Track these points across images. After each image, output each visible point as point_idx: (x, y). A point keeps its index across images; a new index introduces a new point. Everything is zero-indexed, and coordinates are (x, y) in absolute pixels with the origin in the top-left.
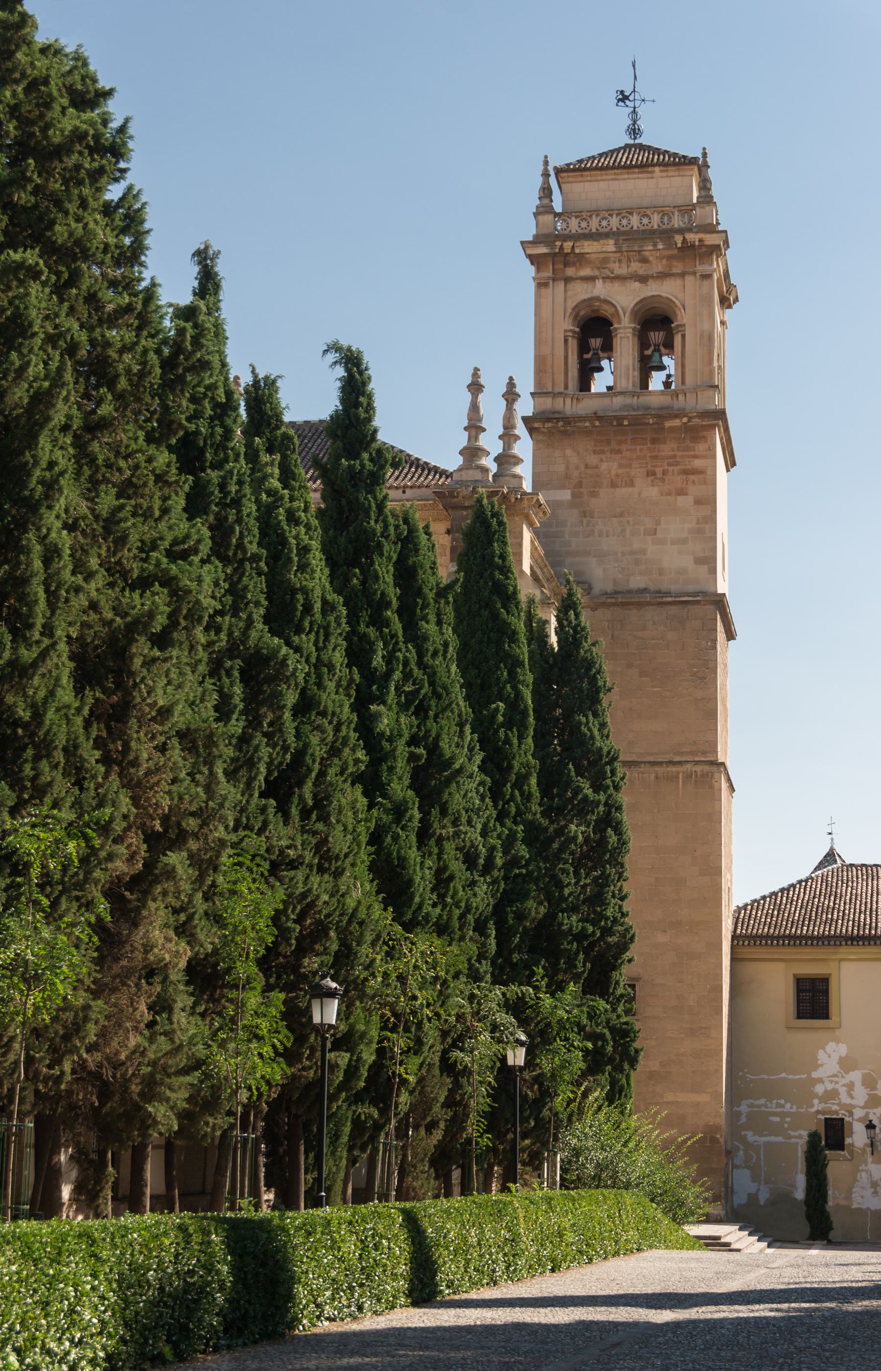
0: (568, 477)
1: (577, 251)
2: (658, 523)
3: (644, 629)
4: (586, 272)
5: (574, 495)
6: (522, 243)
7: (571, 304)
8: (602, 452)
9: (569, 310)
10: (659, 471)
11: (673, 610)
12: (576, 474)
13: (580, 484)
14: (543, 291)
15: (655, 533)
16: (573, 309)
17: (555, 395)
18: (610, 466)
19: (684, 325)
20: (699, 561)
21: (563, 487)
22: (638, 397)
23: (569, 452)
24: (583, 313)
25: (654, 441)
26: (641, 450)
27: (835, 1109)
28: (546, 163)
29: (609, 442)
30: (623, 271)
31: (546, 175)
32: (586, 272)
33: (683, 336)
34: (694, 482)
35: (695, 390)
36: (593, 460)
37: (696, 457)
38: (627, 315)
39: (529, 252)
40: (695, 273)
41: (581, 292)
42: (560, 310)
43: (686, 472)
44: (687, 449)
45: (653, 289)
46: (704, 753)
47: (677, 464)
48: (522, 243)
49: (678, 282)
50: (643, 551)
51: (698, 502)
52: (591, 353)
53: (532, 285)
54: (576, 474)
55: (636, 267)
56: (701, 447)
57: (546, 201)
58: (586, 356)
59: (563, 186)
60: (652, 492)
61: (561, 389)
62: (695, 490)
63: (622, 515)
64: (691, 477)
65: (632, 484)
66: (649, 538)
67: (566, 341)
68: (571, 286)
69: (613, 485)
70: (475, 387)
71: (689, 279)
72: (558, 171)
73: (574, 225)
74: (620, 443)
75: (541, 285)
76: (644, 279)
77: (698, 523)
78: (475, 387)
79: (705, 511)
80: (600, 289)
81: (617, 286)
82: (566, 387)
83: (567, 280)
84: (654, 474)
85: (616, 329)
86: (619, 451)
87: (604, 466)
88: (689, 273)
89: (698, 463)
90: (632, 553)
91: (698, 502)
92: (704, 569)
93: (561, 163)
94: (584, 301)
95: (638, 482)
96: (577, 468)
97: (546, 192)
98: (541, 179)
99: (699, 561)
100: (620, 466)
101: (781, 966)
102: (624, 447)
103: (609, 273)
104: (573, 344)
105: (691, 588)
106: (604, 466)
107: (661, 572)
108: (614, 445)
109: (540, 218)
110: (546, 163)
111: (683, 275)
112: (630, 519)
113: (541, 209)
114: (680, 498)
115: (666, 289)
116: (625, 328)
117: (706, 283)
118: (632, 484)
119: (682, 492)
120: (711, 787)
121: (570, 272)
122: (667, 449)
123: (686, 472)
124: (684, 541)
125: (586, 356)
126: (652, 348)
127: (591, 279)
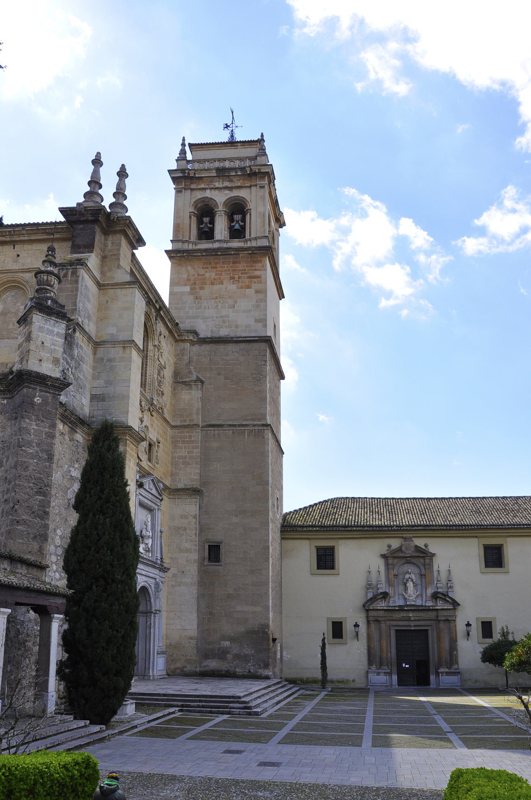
0: (188, 280)
2: (236, 302)
3: (227, 355)
5: (191, 289)
6: (169, 171)
7: (193, 200)
8: (207, 268)
9: (192, 203)
10: (236, 277)
11: (242, 346)
12: (192, 278)
13: (195, 284)
14: (179, 194)
15: (234, 307)
16: (194, 202)
17: (183, 242)
18: (211, 274)
19: (251, 209)
20: (257, 321)
21: (186, 285)
22: (227, 243)
23: (189, 268)
24: (199, 205)
25: (234, 263)
26: (227, 267)
27: (337, 616)
28: (184, 139)
31: (183, 145)
33: (250, 214)
34: (255, 282)
35: (256, 239)
36: (202, 272)
37: (256, 270)
38: (222, 205)
39: (173, 176)
40: (256, 185)
41: (199, 195)
43: (250, 277)
44: (251, 266)
45: (236, 193)
46: (259, 420)
47: (246, 273)
48: (170, 171)
49: (248, 190)
50: (228, 316)
51: (257, 292)
52: (204, 224)
53: (174, 192)
54: (192, 278)
56: (258, 266)
57: (183, 156)
58: (201, 226)
59: (193, 152)
60: (233, 287)
62: (255, 286)
63: (216, 298)
64: (254, 280)
65: (222, 284)
66: (231, 310)
67: (190, 217)
69: (212, 284)
70: (97, 162)
71: (253, 189)
72: (190, 145)
73: (197, 166)
74: (216, 263)
75: (178, 191)
76: (230, 189)
77: (257, 302)
78: (97, 162)
79: (261, 296)
80: (208, 194)
81: (217, 192)
82: (190, 239)
83: (192, 190)
84: (234, 278)
85: (216, 212)
87: (207, 275)
88: (253, 186)
89: (257, 273)
90: (222, 317)
91: (257, 292)
92: (260, 324)
93: (192, 142)
94: (200, 199)
95: (225, 282)
96: (193, 275)
97: (183, 152)
98: (181, 147)
99: (257, 321)
100: (216, 275)
101: (307, 542)
102: (218, 266)
103: (213, 187)
104: (194, 219)
105: (253, 335)
106: (207, 275)
107: (237, 326)
108: (213, 265)
109: (179, 162)
110: (184, 139)
111: (250, 187)
112: (221, 300)
113: (180, 158)
114: (247, 290)
115: (243, 193)
116: (220, 211)
117: (262, 190)
118: (222, 284)
119: (249, 287)
120: (263, 437)
121: (193, 186)
122: (241, 266)
123: (250, 277)
124: (249, 311)
125: (201, 226)
126: (235, 222)
127: (205, 189)
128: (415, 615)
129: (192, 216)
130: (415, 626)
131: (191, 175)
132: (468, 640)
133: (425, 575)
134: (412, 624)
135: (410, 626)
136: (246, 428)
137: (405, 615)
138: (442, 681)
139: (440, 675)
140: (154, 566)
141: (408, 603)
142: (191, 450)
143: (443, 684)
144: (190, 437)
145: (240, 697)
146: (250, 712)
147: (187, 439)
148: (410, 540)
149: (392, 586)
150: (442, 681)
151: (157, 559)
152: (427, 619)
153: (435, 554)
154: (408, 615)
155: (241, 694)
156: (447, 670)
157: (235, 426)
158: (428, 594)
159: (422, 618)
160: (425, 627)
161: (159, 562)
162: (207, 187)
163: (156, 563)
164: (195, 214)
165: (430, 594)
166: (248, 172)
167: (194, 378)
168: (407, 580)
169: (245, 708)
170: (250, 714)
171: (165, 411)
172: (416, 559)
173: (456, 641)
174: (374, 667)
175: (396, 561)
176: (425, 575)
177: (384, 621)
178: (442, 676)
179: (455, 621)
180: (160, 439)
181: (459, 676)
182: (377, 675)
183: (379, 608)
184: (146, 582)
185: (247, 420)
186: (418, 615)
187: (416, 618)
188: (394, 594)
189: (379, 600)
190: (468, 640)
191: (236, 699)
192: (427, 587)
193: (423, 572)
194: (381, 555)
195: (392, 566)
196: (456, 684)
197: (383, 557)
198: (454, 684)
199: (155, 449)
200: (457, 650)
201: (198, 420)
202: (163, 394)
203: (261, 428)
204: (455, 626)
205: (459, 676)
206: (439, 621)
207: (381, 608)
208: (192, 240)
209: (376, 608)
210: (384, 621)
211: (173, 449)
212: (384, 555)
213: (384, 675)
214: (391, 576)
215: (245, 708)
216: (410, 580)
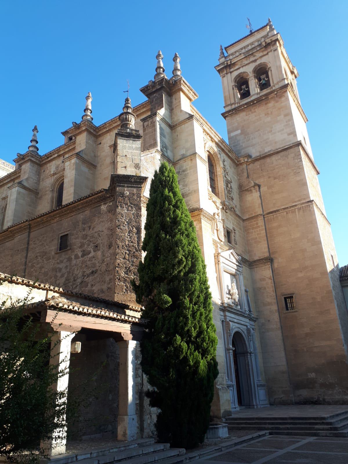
1: (232, 63)
4: (237, 67)
14: (224, 78)
16: (234, 79)
19: (271, 67)
24: (237, 80)
29: (251, 110)
30: (246, 62)
32: (237, 67)
33: (271, 70)
35: (278, 83)
38: (251, 73)
39: (218, 69)
41: (236, 73)
42: (230, 81)
55: (252, 59)
61: (233, 101)
68: (232, 74)
80: (242, 70)
81: (247, 66)
83: (231, 73)
85: (248, 79)
86: (255, 112)
126: (262, 80)
129: (234, 88)
131: (229, 64)
136: (296, 208)
140: (243, 315)
142: (259, 232)
144: (257, 224)
145: (324, 418)
146: (336, 433)
147: (255, 226)
151: (245, 311)
155: (326, 416)
157: (287, 208)
161: (247, 312)
162: (240, 66)
163: (244, 313)
164: (236, 86)
166: (264, 45)
167: (253, 184)
169: (331, 429)
170: (337, 436)
171: (236, 210)
180: (236, 228)
184: (239, 328)
185: (295, 202)
191: (321, 420)
199: (232, 235)
201: (259, 211)
202: (233, 199)
203: (307, 204)
208: (237, 102)
211: (247, 234)
215: (331, 429)
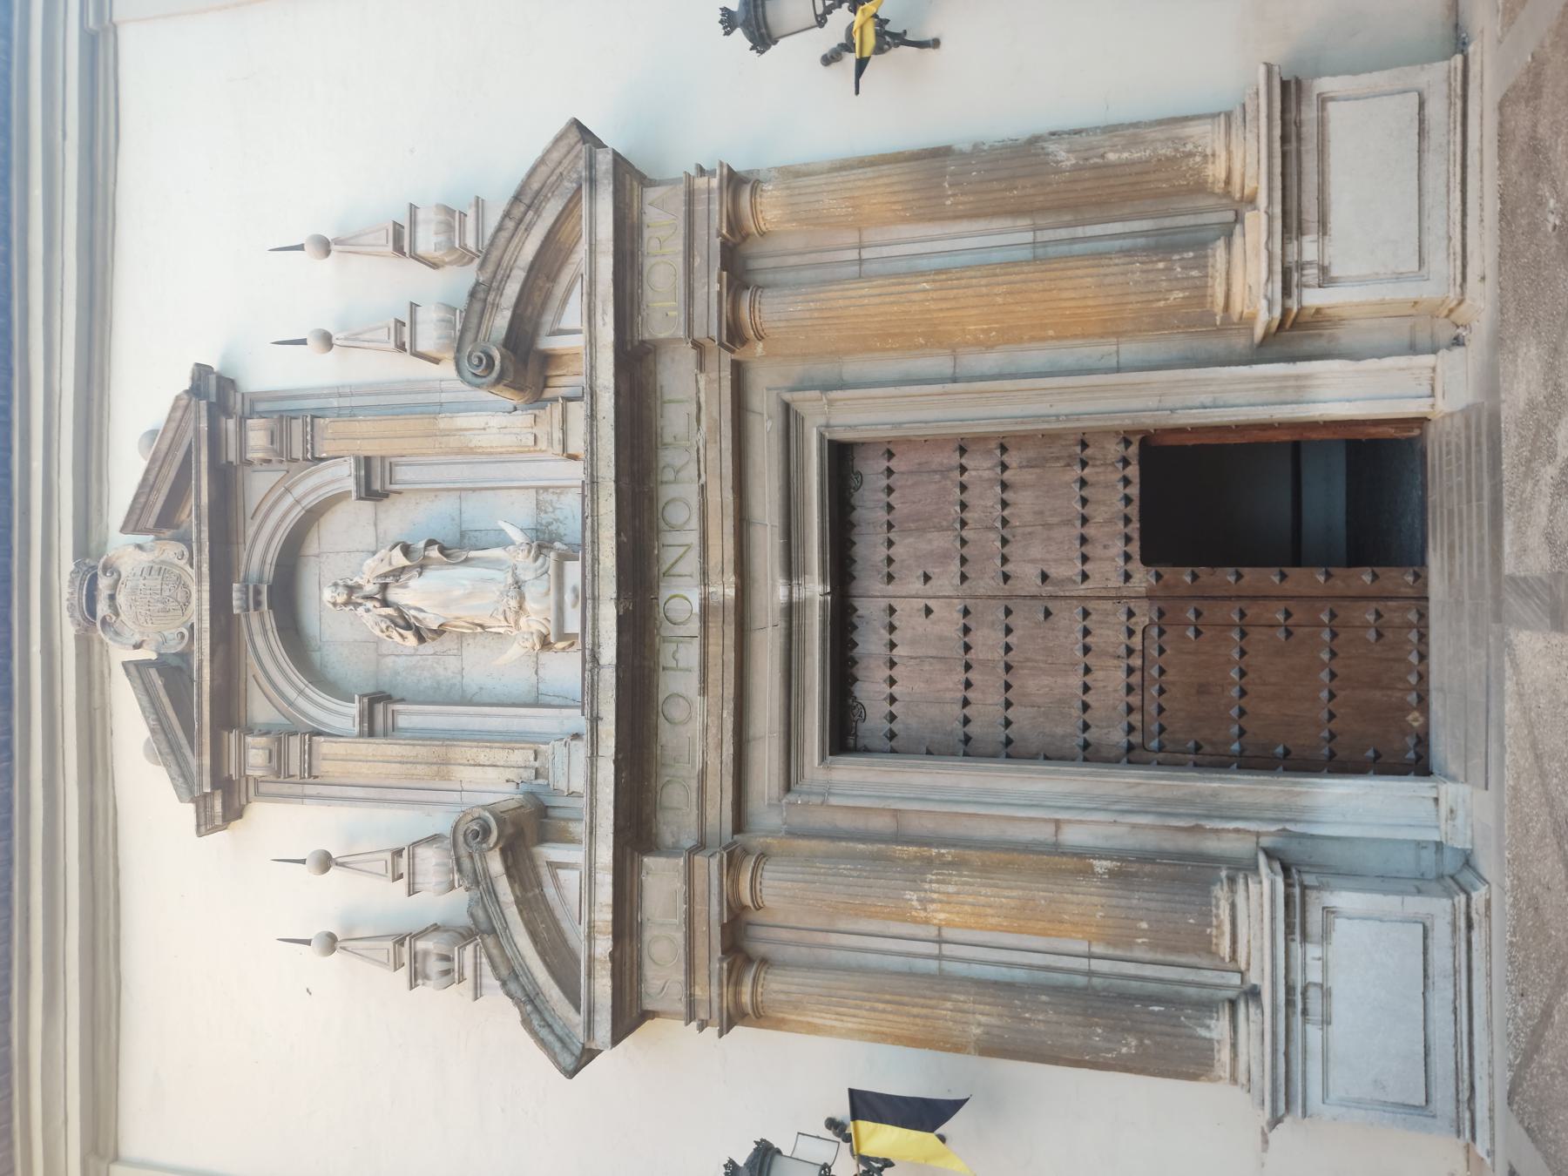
128: (691, 564)
130: (791, 568)
132: (935, 43)
133: (366, 463)
134: (772, 592)
135: (791, 611)
137: (690, 655)
138: (1398, 277)
139: (1313, 298)
141: (573, 625)
143: (1441, 265)
148: (104, 583)
149: (446, 762)
150: (1398, 277)
152: (727, 444)
153: (201, 372)
154: (694, 627)
156: (1257, 227)
158: (509, 440)
159: (721, 496)
160: (802, 469)
165: (522, 419)
168: (404, 623)
172: (251, 531)
173: (940, 153)
174: (1219, 1028)
175: (260, 710)
176: (366, 463)
177: (733, 861)
178: (1326, 278)
179: (735, 182)
181: (1325, 84)
182: (1326, 1021)
183: (604, 916)
186: (693, 538)
187: (722, 547)
188: (510, 739)
189: (550, 891)
190: (935, 43)
192: (453, 442)
193: (342, 476)
194: (205, 825)
195: (295, 742)
196: (1437, 109)
197: (233, 812)
198: (1436, 136)
200: (1035, 140)
204: (792, 174)
205: (1325, 84)
206: (735, 335)
207: (605, 893)
209: (604, 945)
210: (733, 861)
212: (202, 803)
213: (1326, 936)
214: (376, 758)
216: (395, 595)
